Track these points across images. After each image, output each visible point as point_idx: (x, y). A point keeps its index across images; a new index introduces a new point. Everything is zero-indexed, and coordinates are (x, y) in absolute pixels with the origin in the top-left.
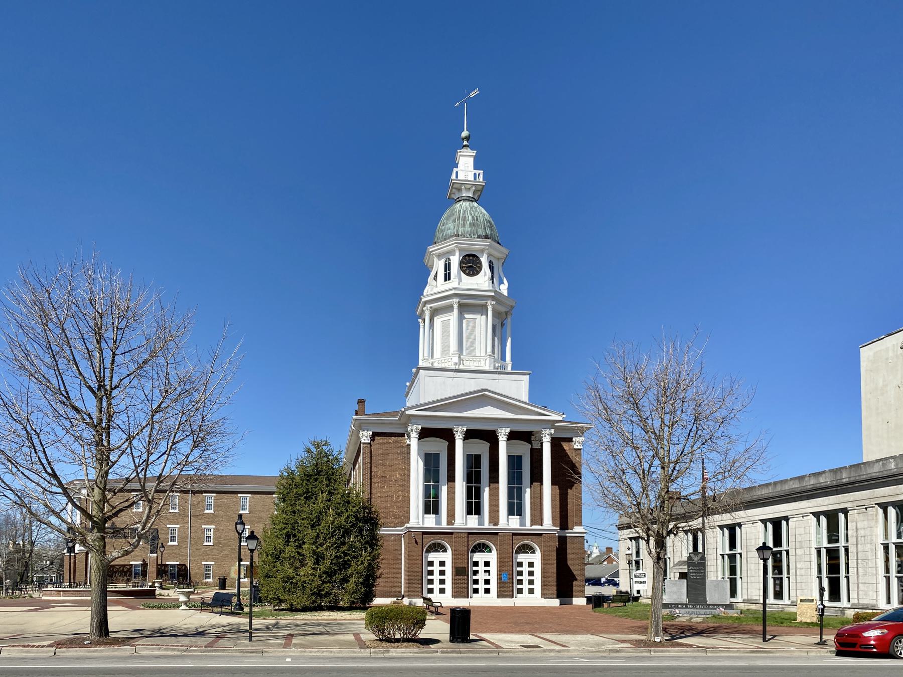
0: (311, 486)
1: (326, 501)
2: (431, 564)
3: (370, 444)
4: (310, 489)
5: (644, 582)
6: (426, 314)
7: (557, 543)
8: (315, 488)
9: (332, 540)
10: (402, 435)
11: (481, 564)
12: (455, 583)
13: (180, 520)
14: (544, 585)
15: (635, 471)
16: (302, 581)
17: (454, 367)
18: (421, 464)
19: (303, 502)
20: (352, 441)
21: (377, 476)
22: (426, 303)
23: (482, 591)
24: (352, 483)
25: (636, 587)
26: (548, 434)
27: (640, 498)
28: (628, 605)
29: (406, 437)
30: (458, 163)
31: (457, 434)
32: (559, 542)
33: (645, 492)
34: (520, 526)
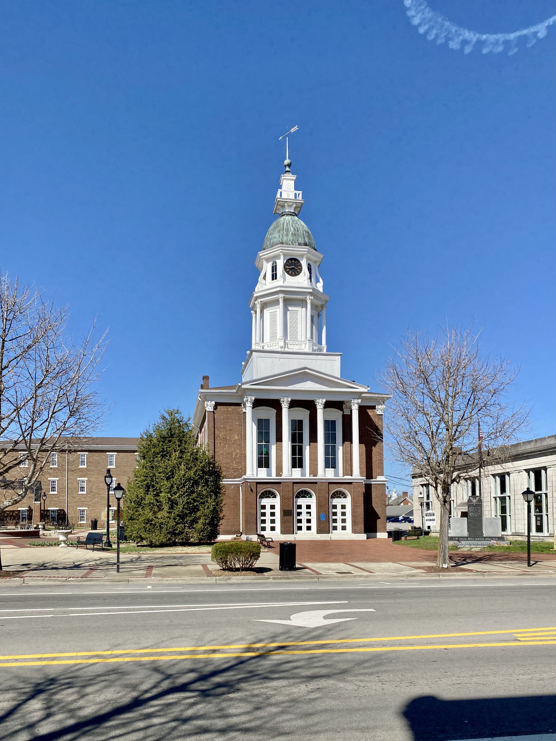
0: (165, 447)
1: (178, 458)
2: (264, 507)
3: (213, 412)
4: (165, 449)
5: (434, 520)
6: (258, 307)
7: (364, 490)
8: (169, 448)
9: (184, 490)
10: (239, 405)
11: (304, 507)
12: (283, 522)
13: (59, 474)
14: (354, 523)
15: (426, 433)
16: (159, 522)
17: (280, 349)
18: (255, 428)
19: (160, 459)
20: (199, 409)
21: (220, 437)
22: (257, 298)
23: (304, 528)
24: (199, 443)
25: (427, 524)
26: (356, 403)
27: (430, 454)
28: (421, 538)
29: (243, 407)
30: (282, 185)
31: (283, 403)
32: (365, 489)
33: (434, 449)
34: (334, 477)
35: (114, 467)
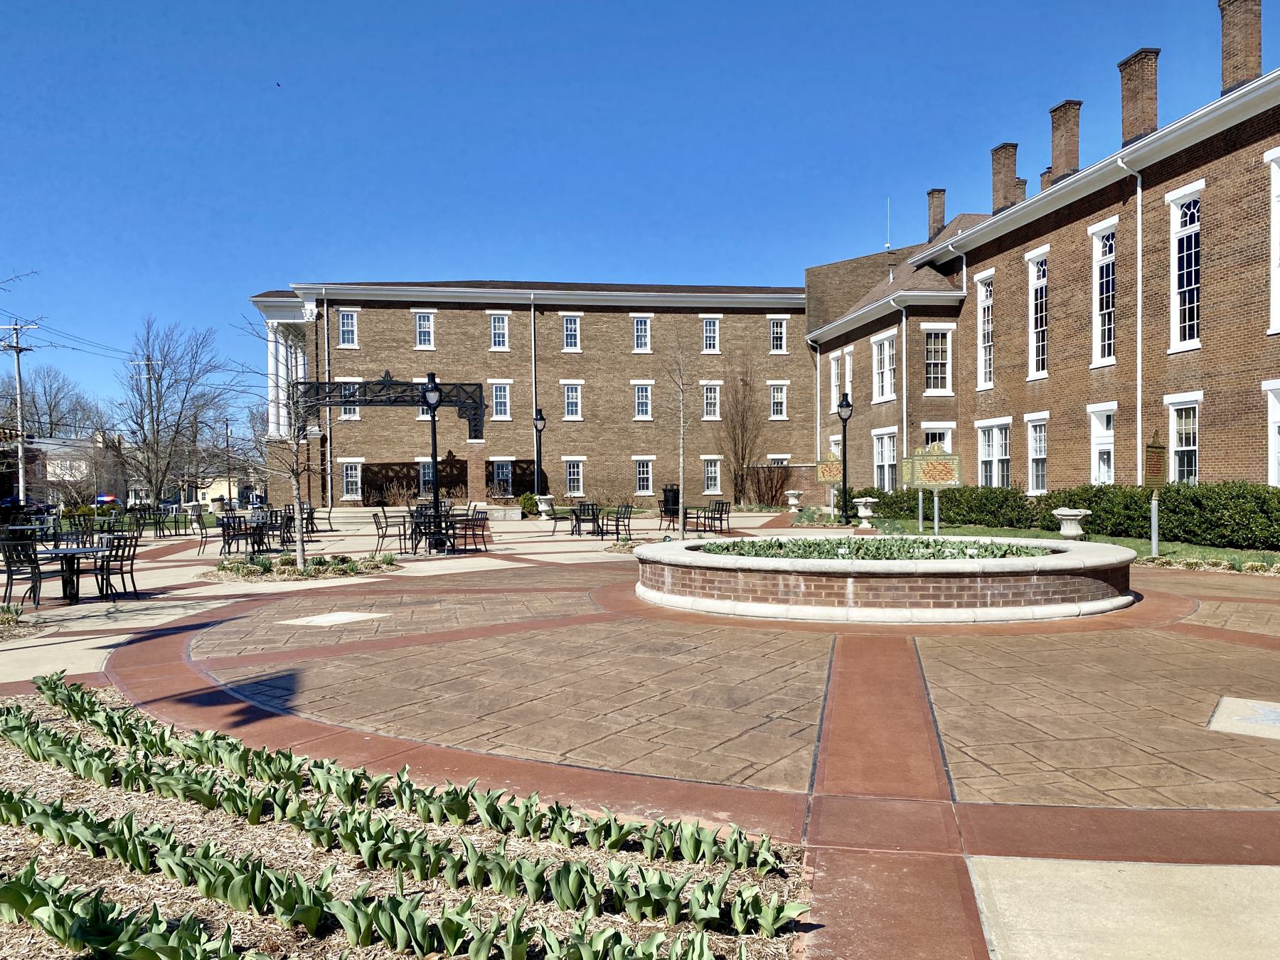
13: (514, 368)
35: (648, 350)
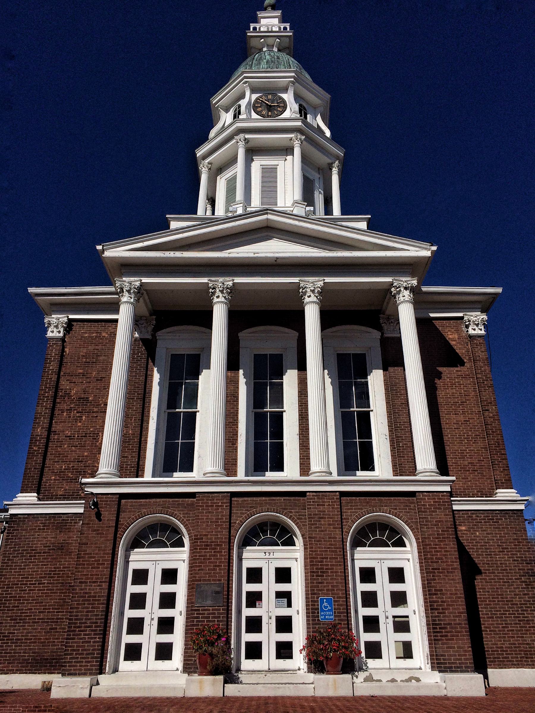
3: (63, 340)
